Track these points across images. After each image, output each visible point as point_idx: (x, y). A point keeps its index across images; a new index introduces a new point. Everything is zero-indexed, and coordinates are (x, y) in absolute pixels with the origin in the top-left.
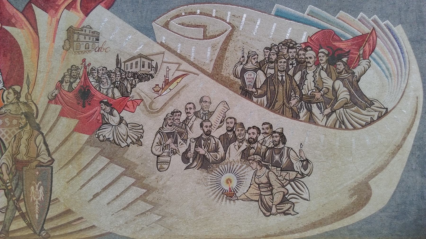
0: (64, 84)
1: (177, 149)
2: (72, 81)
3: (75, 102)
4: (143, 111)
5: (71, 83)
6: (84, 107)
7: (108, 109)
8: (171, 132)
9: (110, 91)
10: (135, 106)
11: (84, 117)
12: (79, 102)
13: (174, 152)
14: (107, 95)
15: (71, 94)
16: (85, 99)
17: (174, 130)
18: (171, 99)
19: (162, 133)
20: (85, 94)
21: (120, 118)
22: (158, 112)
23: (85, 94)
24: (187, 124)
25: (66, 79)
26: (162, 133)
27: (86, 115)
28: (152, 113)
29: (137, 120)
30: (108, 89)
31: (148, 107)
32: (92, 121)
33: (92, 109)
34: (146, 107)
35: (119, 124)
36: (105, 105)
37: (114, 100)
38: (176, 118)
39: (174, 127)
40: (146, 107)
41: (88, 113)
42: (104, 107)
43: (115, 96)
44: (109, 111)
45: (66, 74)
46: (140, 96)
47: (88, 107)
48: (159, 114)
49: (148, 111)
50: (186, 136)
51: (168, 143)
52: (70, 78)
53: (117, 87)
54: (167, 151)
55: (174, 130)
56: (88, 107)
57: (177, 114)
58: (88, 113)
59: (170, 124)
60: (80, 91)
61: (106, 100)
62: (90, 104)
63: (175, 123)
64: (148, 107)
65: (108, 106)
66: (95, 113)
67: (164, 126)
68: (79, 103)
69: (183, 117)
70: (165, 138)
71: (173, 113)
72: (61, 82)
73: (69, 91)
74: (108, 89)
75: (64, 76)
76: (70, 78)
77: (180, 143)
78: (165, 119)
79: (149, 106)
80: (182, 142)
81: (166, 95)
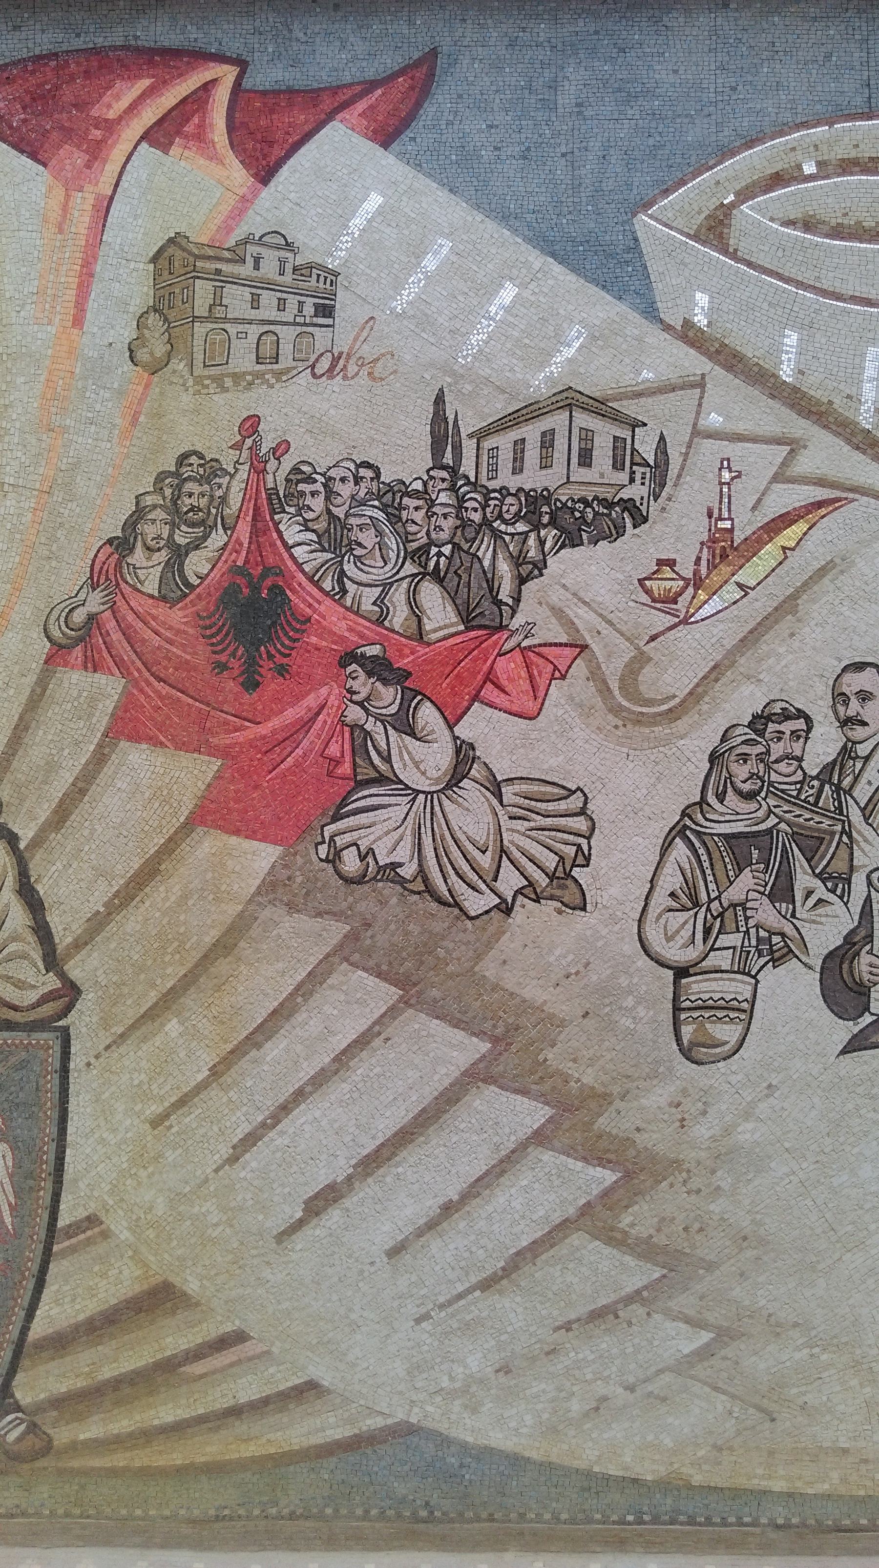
0: (138, 557)
1: (789, 929)
2: (180, 540)
3: (201, 655)
4: (586, 711)
5: (179, 554)
6: (252, 684)
7: (388, 697)
8: (755, 834)
9: (398, 596)
10: (542, 683)
11: (251, 744)
12: (223, 658)
13: (778, 951)
14: (380, 622)
15: (177, 616)
16: (256, 644)
17: (772, 821)
18: (750, 639)
19: (698, 834)
20: (256, 616)
21: (458, 751)
22: (673, 715)
23: (256, 616)
24: (846, 782)
25: (149, 530)
26: (698, 834)
27: (263, 730)
28: (639, 720)
29: (553, 762)
30: (386, 586)
31: (614, 686)
32: (297, 764)
33: (299, 698)
34: (604, 690)
35: (449, 786)
36: (370, 674)
37: (422, 650)
38: (778, 750)
39: (772, 802)
40: (604, 690)
41: (275, 722)
42: (362, 684)
43: (428, 626)
44: (393, 709)
45: (149, 500)
46: (570, 625)
47: (272, 685)
48: (681, 725)
49: (616, 710)
50: (843, 853)
51: (735, 893)
52: (174, 526)
53: (438, 577)
54: (734, 939)
55: (772, 821)
56: (272, 685)
57: (787, 727)
58: (275, 722)
59: (746, 787)
60: (228, 596)
61: (373, 650)
62: (282, 671)
63: (774, 777)
64: (614, 686)
65: (385, 682)
66: (313, 720)
67: (711, 799)
68: (222, 667)
69: (823, 746)
70: (718, 866)
71: (760, 722)
72: (122, 545)
73: (163, 598)
74: (386, 586)
75: (139, 514)
76: (174, 526)
77: (809, 893)
78: (714, 758)
79: (622, 680)
80: (821, 892)
81: (720, 614)
